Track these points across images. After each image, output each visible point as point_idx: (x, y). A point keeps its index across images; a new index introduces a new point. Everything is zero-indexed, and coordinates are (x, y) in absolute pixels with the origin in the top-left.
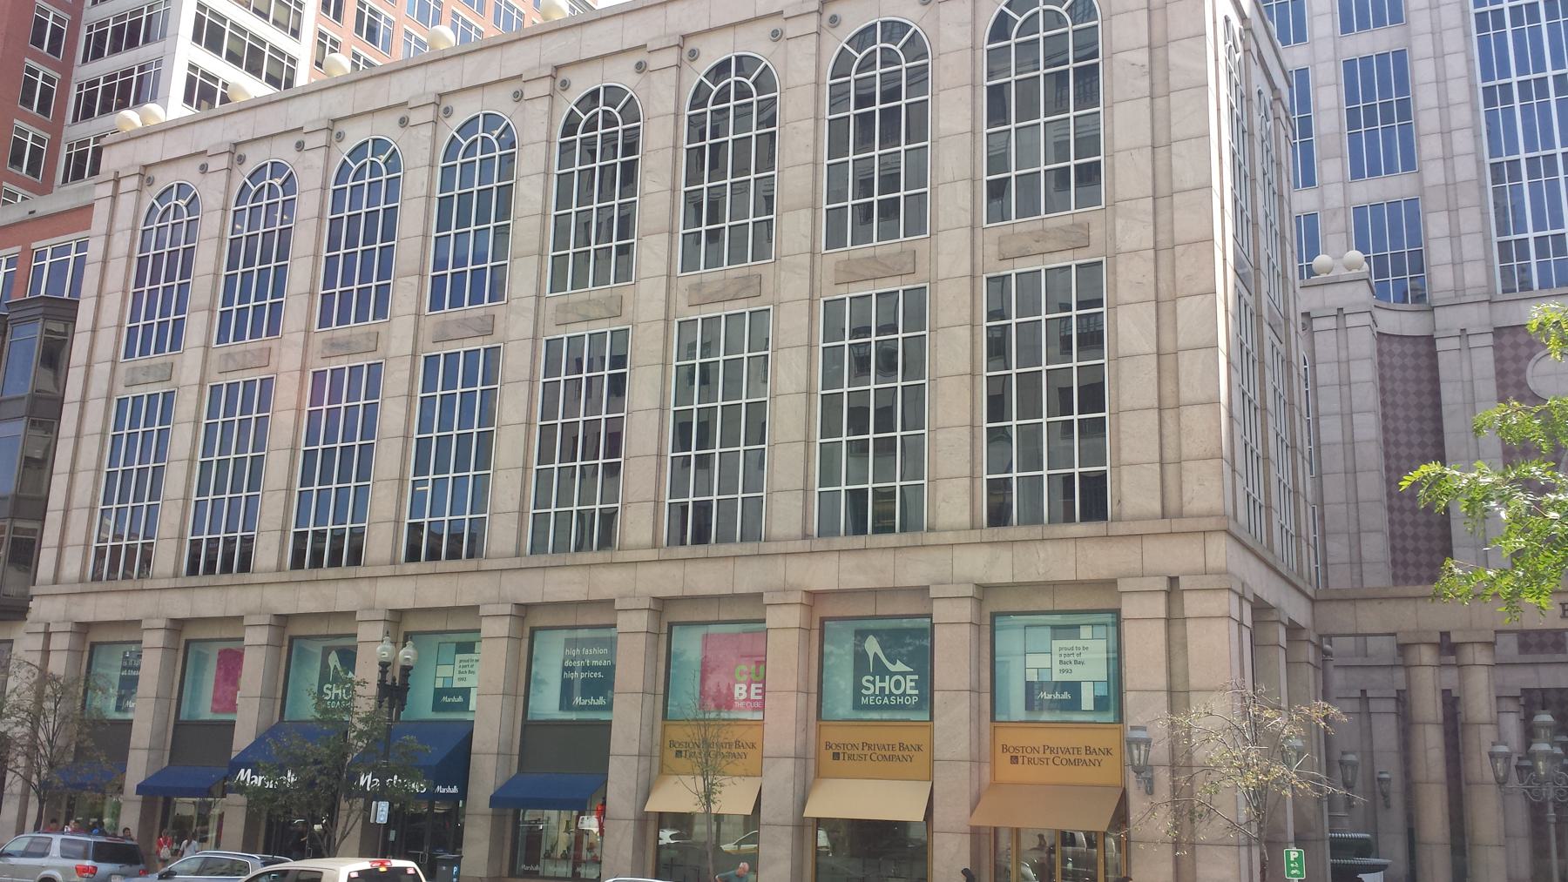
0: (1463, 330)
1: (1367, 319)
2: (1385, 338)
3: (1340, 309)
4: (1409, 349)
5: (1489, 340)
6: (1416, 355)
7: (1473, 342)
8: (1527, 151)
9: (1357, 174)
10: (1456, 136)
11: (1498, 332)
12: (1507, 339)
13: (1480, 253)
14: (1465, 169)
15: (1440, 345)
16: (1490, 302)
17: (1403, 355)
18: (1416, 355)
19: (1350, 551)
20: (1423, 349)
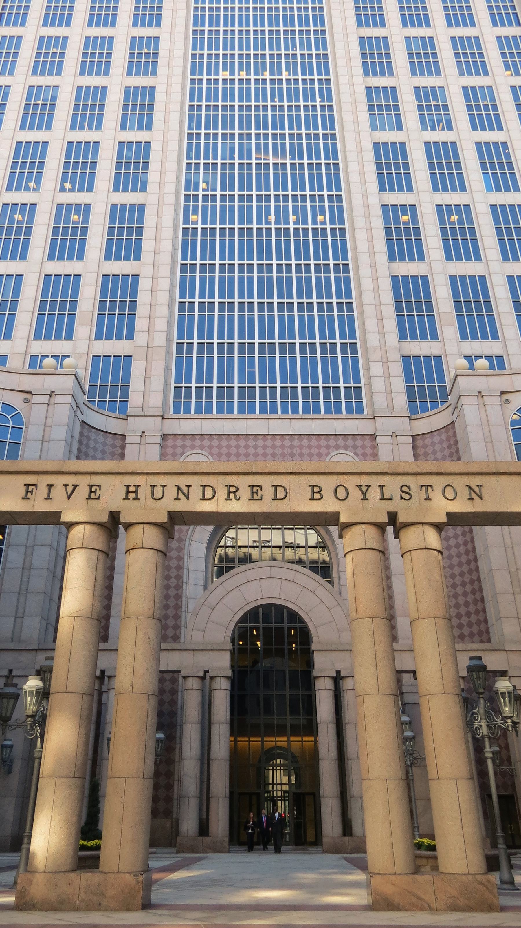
0: (143, 432)
1: (69, 399)
2: (94, 430)
3: (53, 392)
4: (109, 440)
5: (159, 439)
6: (113, 446)
7: (149, 440)
8: (198, 339)
9: (98, 336)
10: (157, 321)
11: (165, 436)
12: (170, 442)
13: (161, 388)
14: (160, 340)
15: (128, 439)
16: (163, 418)
17: (104, 444)
18: (113, 446)
19: (25, 559)
20: (118, 442)
